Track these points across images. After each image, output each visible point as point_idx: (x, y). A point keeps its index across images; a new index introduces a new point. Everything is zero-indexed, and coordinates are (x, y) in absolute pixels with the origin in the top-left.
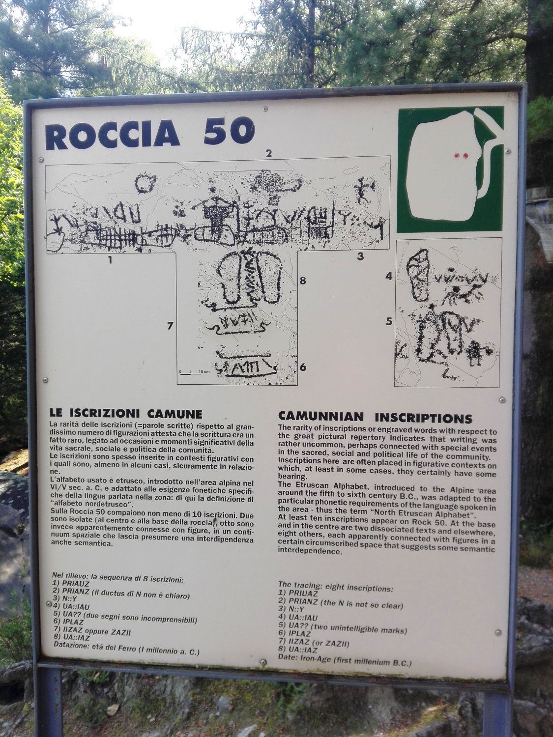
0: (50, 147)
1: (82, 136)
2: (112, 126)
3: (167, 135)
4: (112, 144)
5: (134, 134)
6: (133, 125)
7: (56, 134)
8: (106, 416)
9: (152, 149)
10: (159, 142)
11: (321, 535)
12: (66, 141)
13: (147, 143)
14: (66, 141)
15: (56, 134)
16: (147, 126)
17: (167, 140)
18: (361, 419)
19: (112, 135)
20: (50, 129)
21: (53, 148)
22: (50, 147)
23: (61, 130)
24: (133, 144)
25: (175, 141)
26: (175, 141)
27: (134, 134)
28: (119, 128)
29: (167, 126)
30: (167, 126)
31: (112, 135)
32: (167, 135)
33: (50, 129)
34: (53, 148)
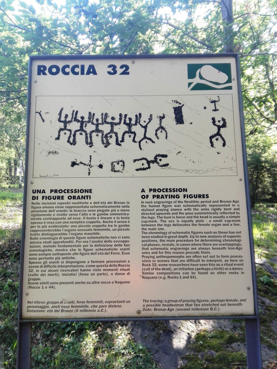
0: (39, 74)
1: (54, 70)
2: (68, 66)
3: (91, 70)
4: (67, 74)
5: (77, 70)
6: (77, 66)
7: (42, 69)
8: (203, 197)
9: (85, 76)
10: (88, 73)
11: (156, 241)
12: (47, 72)
13: (82, 73)
14: (47, 72)
15: (42, 69)
16: (83, 67)
17: (91, 73)
18: (186, 191)
19: (67, 70)
20: (39, 67)
21: (40, 75)
22: (39, 74)
23: (45, 68)
24: (77, 74)
25: (95, 73)
26: (95, 73)
27: (77, 70)
28: (71, 67)
29: (92, 67)
30: (92, 67)
31: (67, 70)
32: (91, 70)
33: (39, 67)
34: (40, 75)
